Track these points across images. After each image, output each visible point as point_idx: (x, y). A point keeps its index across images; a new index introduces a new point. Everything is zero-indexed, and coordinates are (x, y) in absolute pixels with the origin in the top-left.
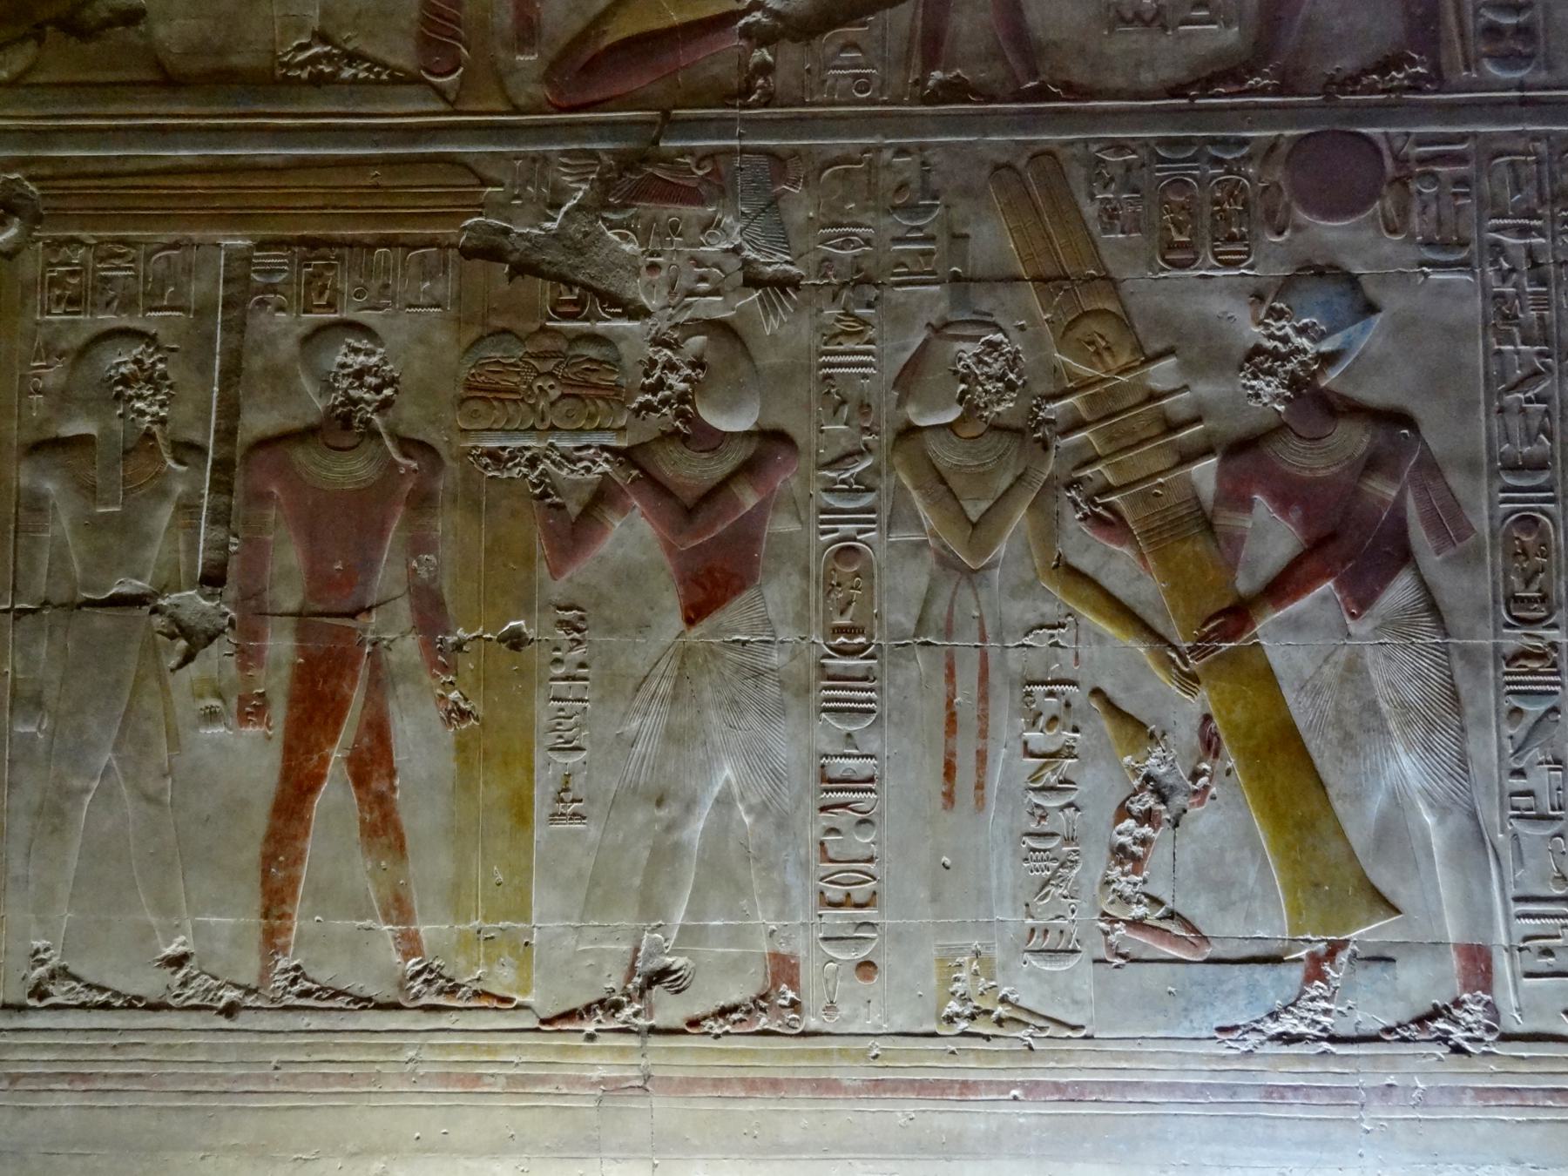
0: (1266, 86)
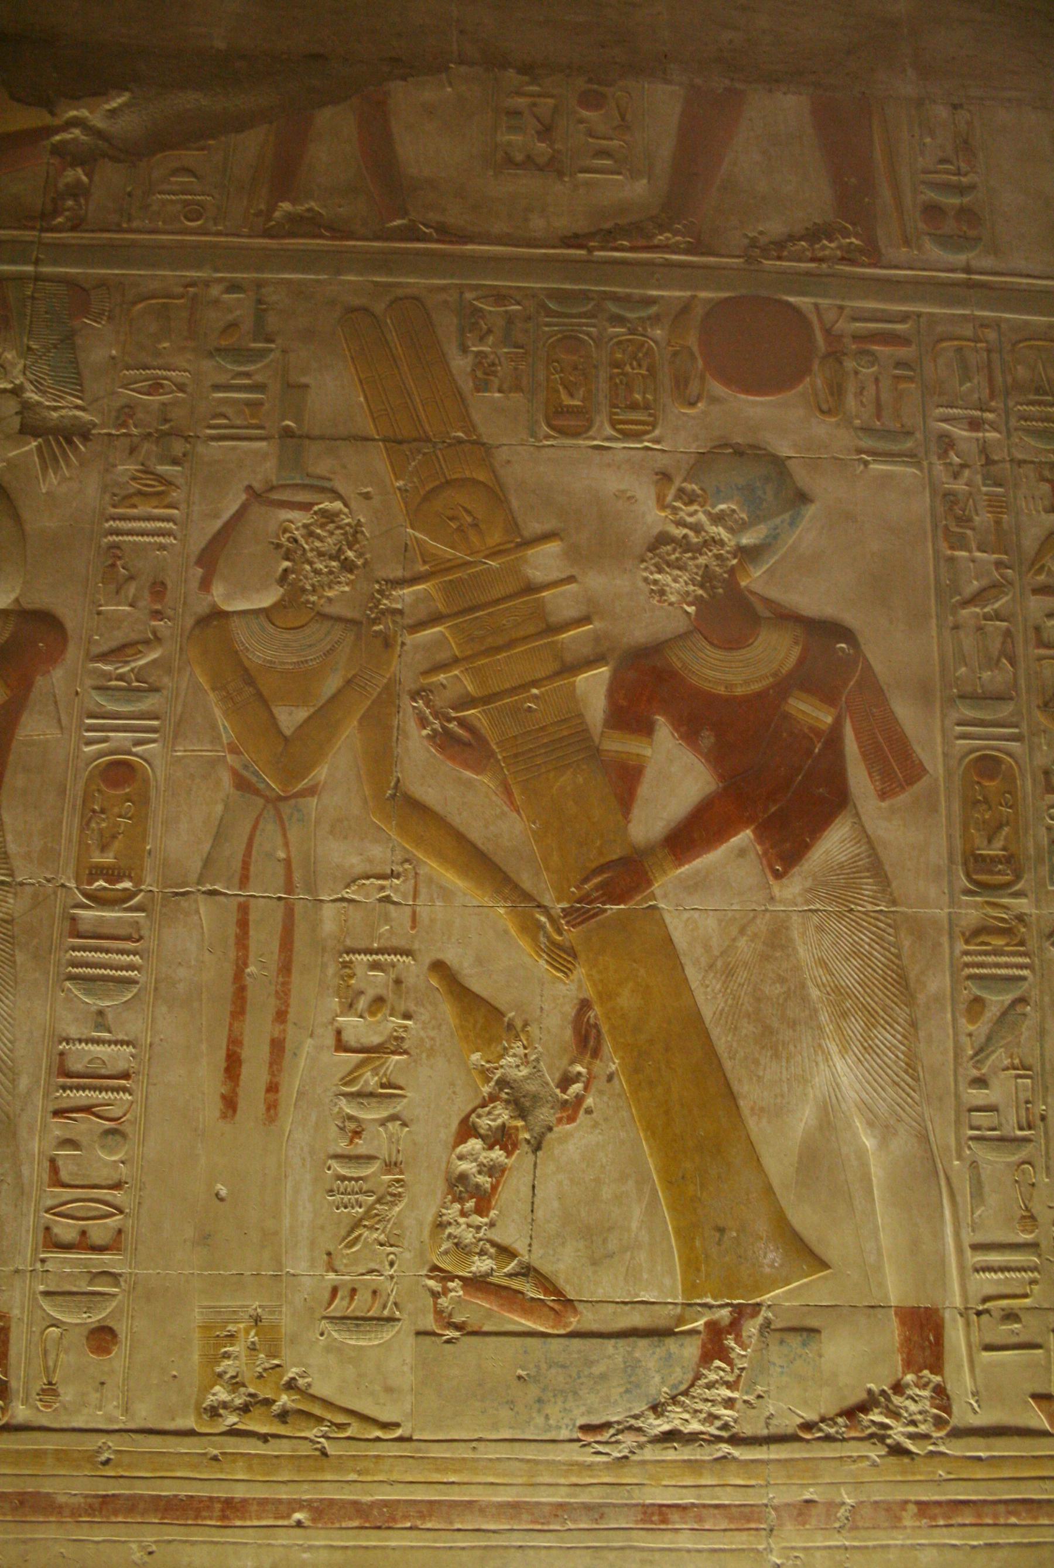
0: (678, 243)
